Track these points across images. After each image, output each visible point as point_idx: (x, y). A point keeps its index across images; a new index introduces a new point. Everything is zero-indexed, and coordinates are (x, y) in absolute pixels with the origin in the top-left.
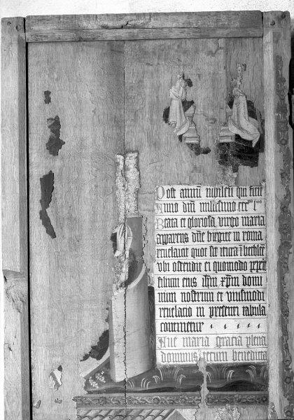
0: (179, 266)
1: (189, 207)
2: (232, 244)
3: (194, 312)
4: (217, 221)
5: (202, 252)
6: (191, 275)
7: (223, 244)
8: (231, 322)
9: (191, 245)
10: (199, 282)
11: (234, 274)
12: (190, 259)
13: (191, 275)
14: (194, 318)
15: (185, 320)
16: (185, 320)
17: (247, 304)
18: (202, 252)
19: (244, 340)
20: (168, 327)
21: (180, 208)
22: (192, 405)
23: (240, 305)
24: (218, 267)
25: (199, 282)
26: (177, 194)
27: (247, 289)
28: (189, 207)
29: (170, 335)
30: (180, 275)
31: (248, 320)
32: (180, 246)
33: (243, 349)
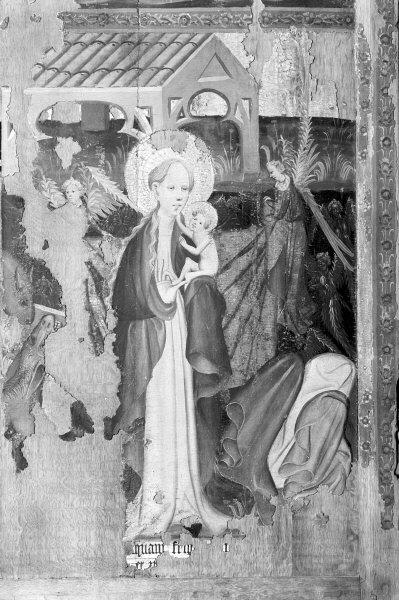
22: (239, 27)
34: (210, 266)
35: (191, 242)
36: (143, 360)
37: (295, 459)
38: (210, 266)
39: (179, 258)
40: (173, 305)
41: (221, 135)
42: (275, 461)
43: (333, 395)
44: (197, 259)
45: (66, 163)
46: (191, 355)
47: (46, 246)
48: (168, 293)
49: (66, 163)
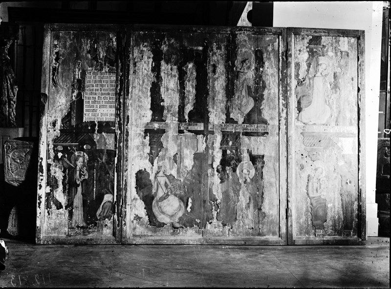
0: (91, 94)
1: (95, 77)
2: (106, 88)
3: (95, 106)
4: (102, 81)
5: (98, 90)
6: (94, 96)
7: (104, 88)
8: (105, 110)
9: (95, 88)
10: (97, 98)
11: (107, 96)
12: (94, 92)
13: (94, 96)
14: (95, 108)
15: (92, 109)
16: (92, 109)
17: (110, 105)
18: (98, 90)
19: (109, 115)
20: (87, 111)
21: (92, 77)
23: (108, 105)
24: (102, 94)
25: (97, 98)
26: (92, 74)
27: (110, 100)
28: (95, 77)
29: (88, 113)
30: (91, 96)
31: (110, 109)
32: (92, 88)
33: (108, 117)
34: (86, 177)
35: (83, 172)
36: (73, 194)
37: (102, 214)
38: (86, 177)
39: (80, 175)
40: (79, 185)
41: (89, 152)
42: (98, 213)
43: (109, 202)
44: (84, 175)
45: (60, 157)
46: (82, 194)
47: (55, 173)
48: (78, 183)
49: (60, 157)
